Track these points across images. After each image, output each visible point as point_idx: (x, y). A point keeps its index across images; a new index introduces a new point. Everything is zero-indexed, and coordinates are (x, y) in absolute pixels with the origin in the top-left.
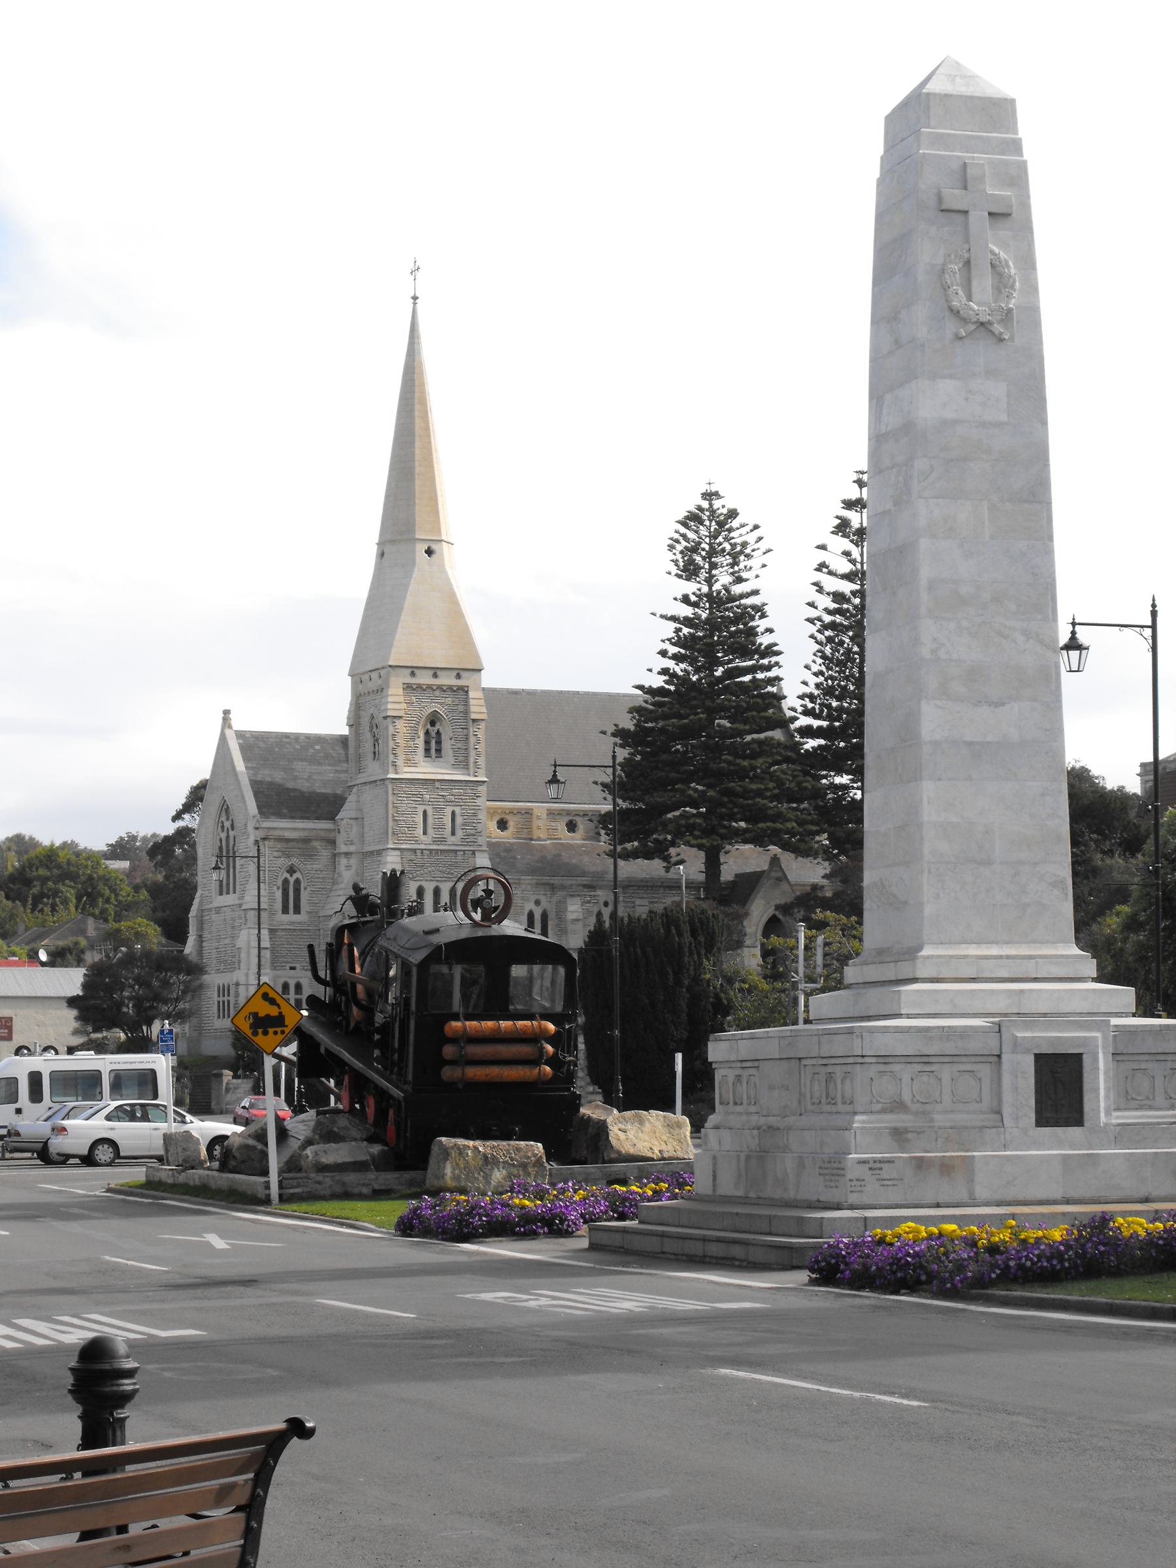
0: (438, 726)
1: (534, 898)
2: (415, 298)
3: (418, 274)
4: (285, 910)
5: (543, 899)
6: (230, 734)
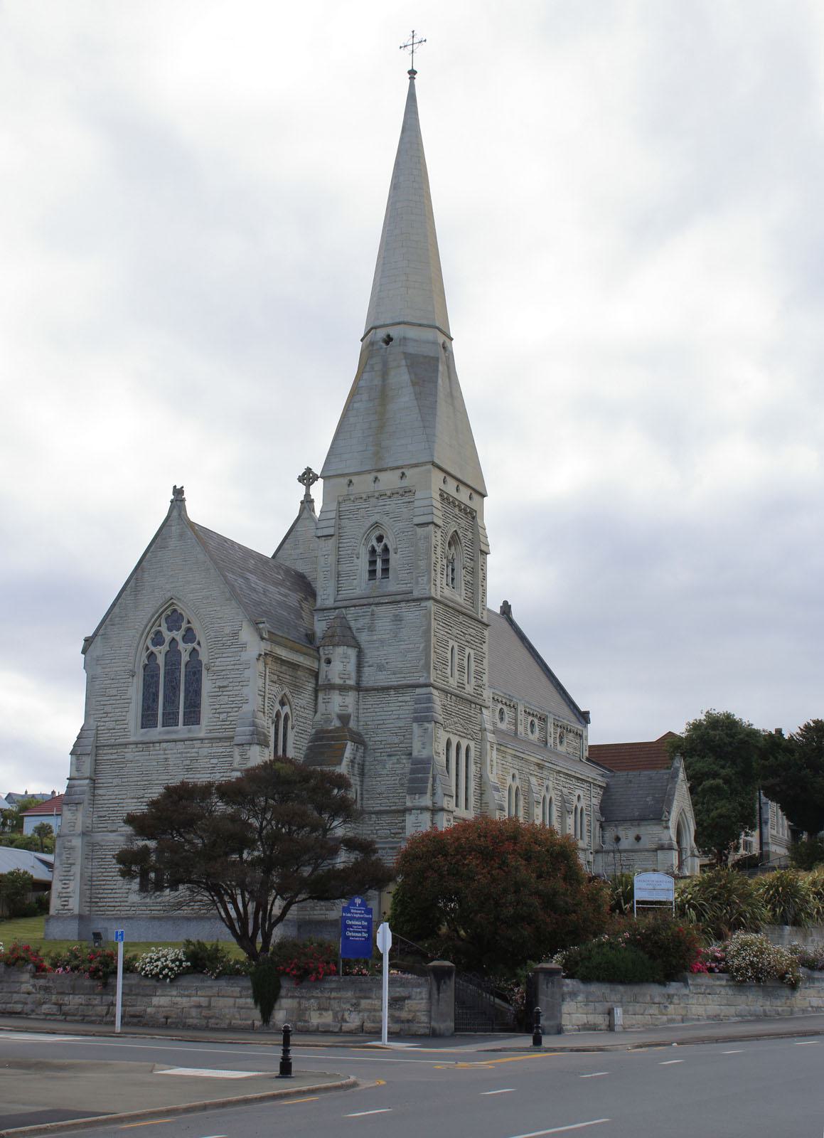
1: (512, 771)
2: (412, 73)
3: (419, 49)
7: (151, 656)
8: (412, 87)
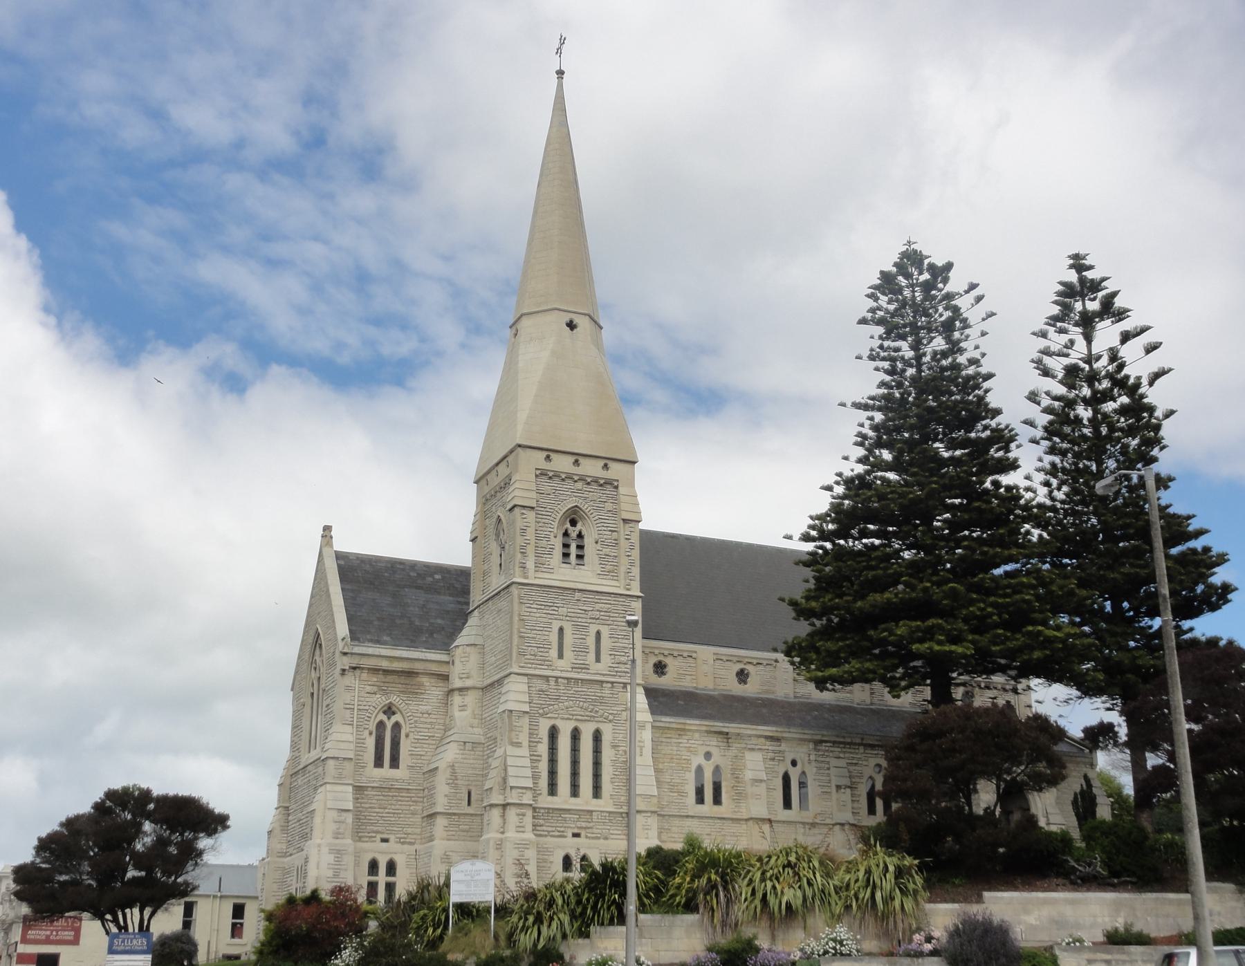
0: (579, 526)
2: (560, 73)
4: (379, 762)
5: (715, 751)
6: (326, 551)
8: (560, 87)
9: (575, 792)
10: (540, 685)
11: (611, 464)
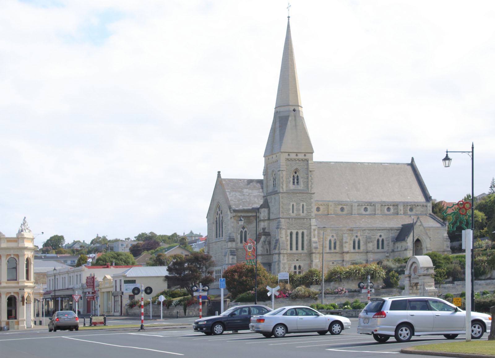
0: (297, 174)
7: (217, 218)
9: (297, 249)
10: (288, 220)
11: (307, 155)
